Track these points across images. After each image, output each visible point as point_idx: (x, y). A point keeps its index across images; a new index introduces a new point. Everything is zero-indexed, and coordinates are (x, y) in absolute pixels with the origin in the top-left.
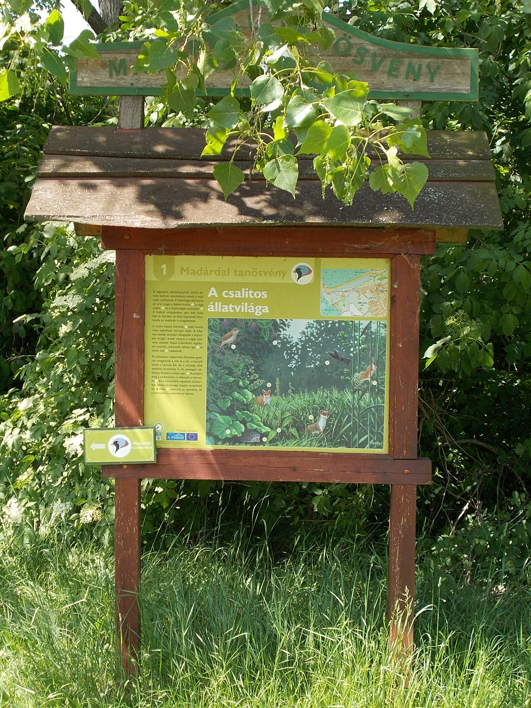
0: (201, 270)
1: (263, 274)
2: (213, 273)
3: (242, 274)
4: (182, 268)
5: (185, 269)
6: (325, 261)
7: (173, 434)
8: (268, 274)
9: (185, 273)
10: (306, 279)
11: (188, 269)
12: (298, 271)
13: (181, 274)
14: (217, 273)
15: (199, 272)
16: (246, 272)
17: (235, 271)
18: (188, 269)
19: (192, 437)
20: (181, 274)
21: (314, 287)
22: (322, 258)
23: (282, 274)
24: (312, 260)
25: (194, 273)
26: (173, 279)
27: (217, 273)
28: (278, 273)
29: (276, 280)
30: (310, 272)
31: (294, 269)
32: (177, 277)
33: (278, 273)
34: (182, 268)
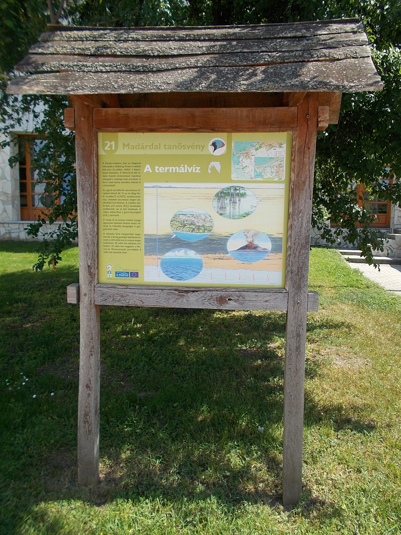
0: (139, 146)
1: (187, 148)
2: (148, 148)
3: (170, 148)
4: (124, 144)
5: (126, 144)
6: (236, 136)
7: (120, 273)
8: (190, 148)
9: (126, 148)
10: (220, 151)
11: (128, 144)
12: (214, 144)
13: (124, 148)
14: (151, 147)
15: (137, 147)
16: (173, 146)
17: (165, 145)
18: (128, 144)
19: (134, 275)
20: (124, 148)
21: (228, 156)
22: (233, 134)
23: (201, 148)
24: (225, 134)
25: (133, 148)
26: (117, 153)
27: (151, 147)
28: (198, 147)
29: (197, 152)
30: (223, 145)
31: (211, 143)
32: (121, 151)
33: (198, 147)
34: (124, 144)
